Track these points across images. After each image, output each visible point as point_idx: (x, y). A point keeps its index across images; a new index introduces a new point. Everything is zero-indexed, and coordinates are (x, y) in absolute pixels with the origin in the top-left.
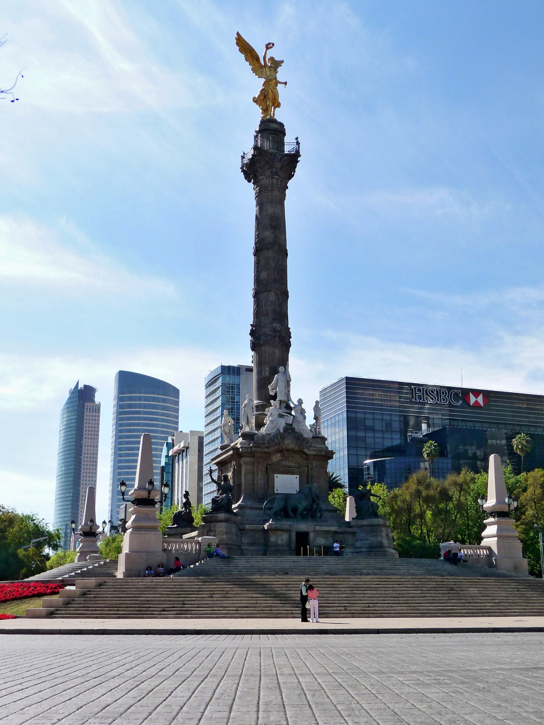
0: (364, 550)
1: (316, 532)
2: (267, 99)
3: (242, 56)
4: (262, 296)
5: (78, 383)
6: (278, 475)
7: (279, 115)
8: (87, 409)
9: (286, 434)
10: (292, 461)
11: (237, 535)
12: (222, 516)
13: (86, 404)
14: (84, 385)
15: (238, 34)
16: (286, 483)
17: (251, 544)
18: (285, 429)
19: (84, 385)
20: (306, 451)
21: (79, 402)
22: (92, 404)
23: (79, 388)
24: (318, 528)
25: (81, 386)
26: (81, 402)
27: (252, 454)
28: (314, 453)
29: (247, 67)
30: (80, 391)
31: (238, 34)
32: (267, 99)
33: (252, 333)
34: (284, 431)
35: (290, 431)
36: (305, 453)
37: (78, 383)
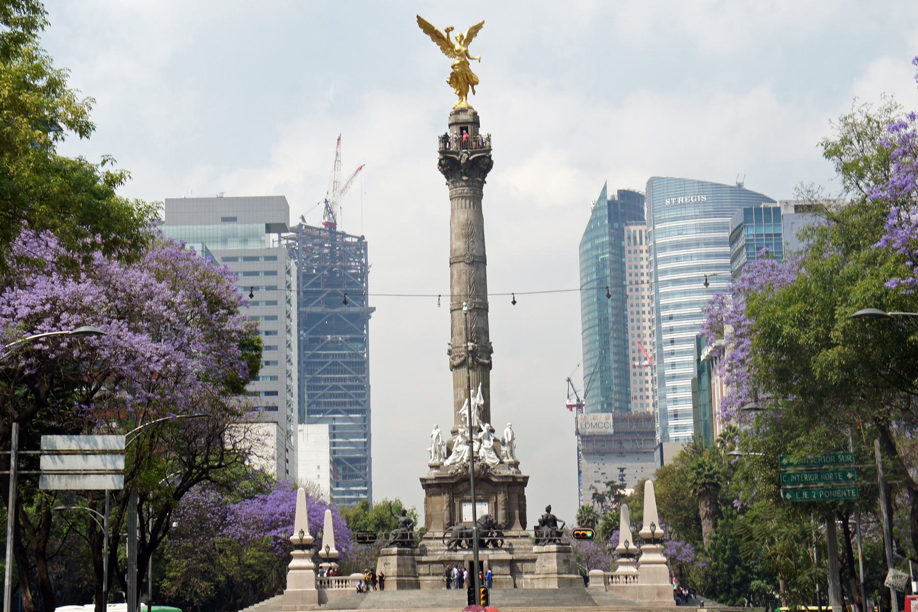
1: (489, 561)
2: (463, 80)
3: (429, 37)
4: (456, 313)
5: (605, 188)
7: (473, 101)
8: (629, 238)
12: (395, 550)
13: (626, 228)
14: (619, 191)
15: (418, 17)
16: (471, 513)
17: (429, 575)
19: (619, 191)
21: (611, 228)
22: (638, 228)
23: (609, 198)
24: (491, 557)
25: (612, 193)
26: (616, 225)
27: (438, 486)
28: (501, 480)
29: (435, 47)
30: (611, 204)
31: (418, 17)
32: (463, 80)
33: (450, 352)
37: (605, 188)
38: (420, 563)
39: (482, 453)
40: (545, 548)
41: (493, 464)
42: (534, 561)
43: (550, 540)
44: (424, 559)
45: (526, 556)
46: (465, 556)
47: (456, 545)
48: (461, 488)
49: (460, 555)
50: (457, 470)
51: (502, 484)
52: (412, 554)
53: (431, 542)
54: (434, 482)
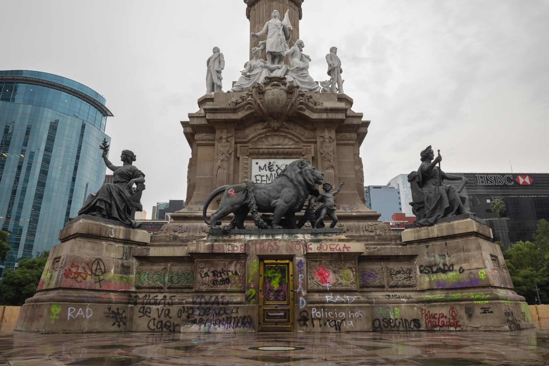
0: (439, 295)
6: (257, 161)
9: (269, 87)
10: (285, 137)
11: (125, 269)
17: (160, 289)
18: (270, 80)
20: (307, 113)
24: (314, 248)
28: (324, 116)
34: (266, 84)
35: (275, 82)
36: (307, 120)
38: (144, 259)
39: (289, 78)
40: (435, 231)
41: (311, 90)
42: (411, 258)
43: (447, 211)
44: (154, 252)
45: (390, 249)
46: (246, 245)
47: (233, 225)
48: (251, 132)
49: (237, 244)
50: (243, 98)
51: (328, 124)
52: (126, 241)
53: (186, 224)
54: (203, 122)
